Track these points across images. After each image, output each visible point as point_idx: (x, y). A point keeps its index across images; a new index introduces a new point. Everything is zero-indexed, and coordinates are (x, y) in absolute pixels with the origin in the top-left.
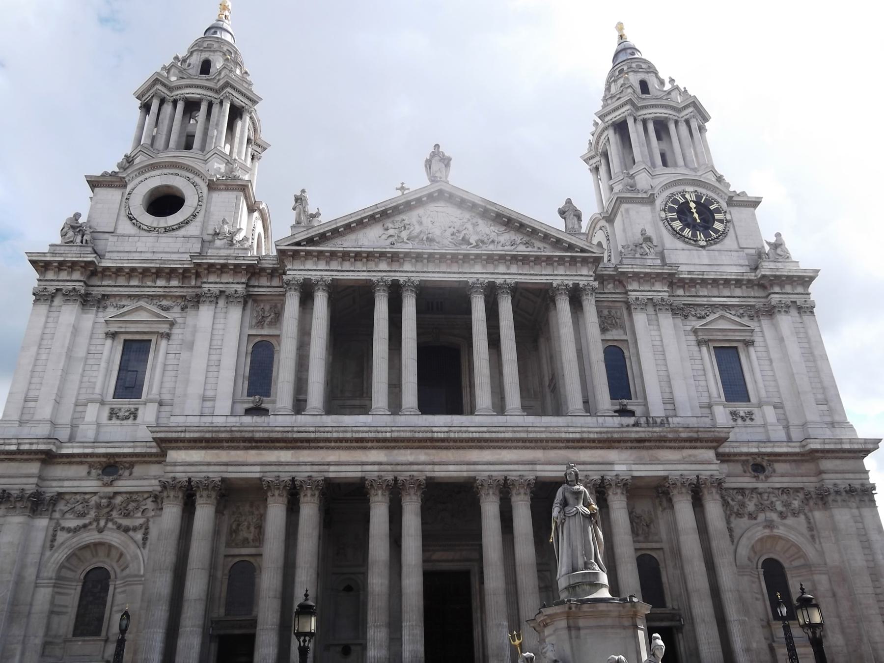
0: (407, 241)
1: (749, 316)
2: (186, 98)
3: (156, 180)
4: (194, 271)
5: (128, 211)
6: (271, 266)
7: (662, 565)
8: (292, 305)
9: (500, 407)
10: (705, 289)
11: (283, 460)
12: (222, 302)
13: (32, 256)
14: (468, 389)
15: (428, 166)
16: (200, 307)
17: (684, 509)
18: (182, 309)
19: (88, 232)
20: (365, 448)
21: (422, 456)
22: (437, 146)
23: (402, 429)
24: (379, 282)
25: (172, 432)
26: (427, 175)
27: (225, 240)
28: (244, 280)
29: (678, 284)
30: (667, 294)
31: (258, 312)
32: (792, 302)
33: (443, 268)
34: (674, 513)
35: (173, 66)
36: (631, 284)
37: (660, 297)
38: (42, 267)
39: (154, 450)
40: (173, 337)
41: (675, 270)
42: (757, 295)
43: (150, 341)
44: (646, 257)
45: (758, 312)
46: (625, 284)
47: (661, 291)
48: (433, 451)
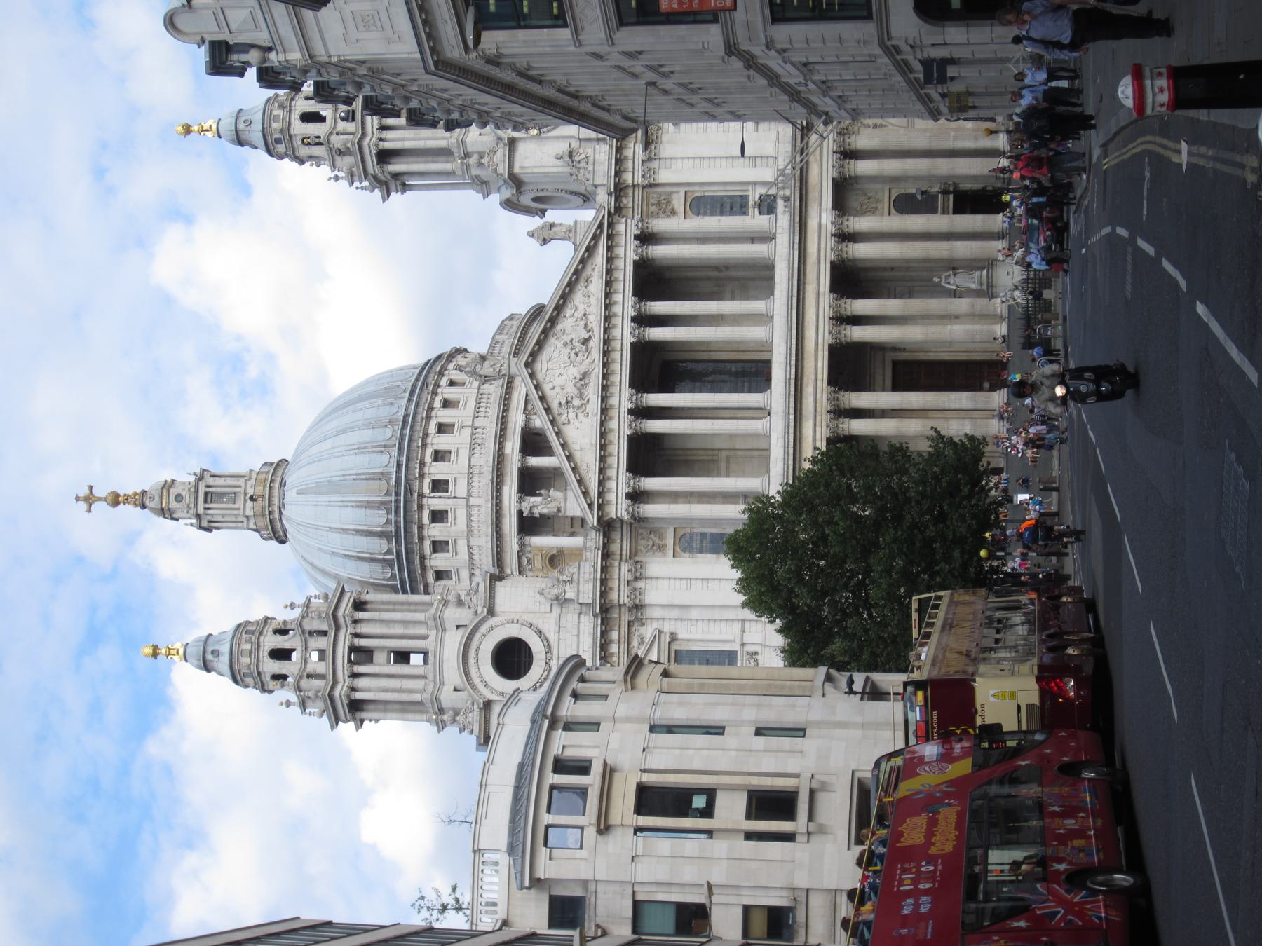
4: (604, 614)
6: (601, 538)
7: (903, 191)
8: (651, 510)
14: (712, 353)
16: (647, 602)
17: (863, 167)
18: (643, 624)
21: (809, 390)
28: (617, 564)
30: (637, 145)
33: (616, 367)
34: (861, 177)
36: (624, 180)
40: (672, 631)
44: (591, 159)
46: (624, 186)
48: (805, 380)
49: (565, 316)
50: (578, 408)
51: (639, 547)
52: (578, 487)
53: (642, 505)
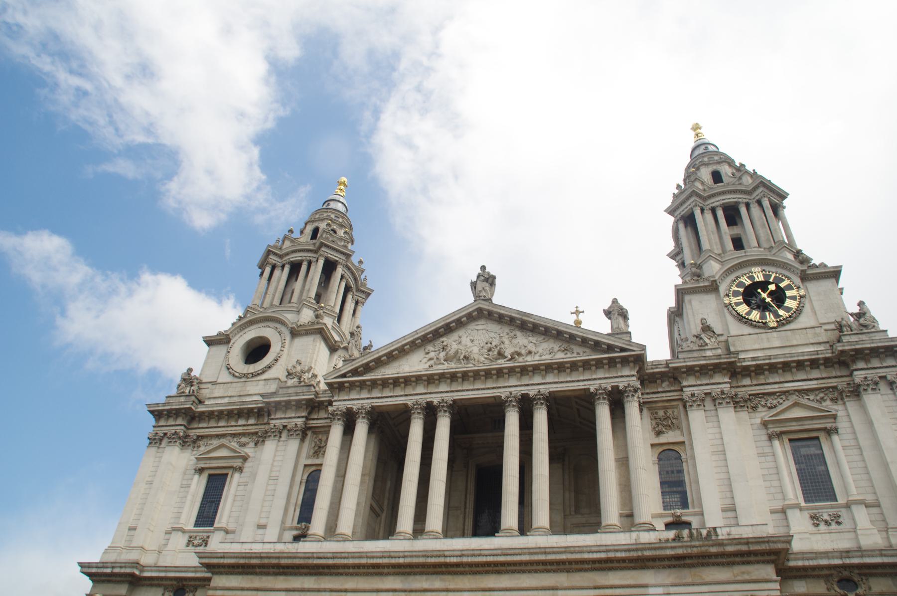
0: (445, 363)
1: (832, 400)
2: (291, 261)
3: (252, 333)
4: (266, 410)
5: (227, 362)
6: (327, 399)
8: (336, 432)
9: (525, 527)
10: (776, 375)
11: (306, 586)
12: (284, 435)
13: (150, 407)
15: (474, 289)
18: (256, 444)
19: (195, 383)
20: (381, 574)
22: (483, 268)
23: (414, 554)
24: (414, 405)
25: (214, 558)
26: (474, 296)
27: (296, 380)
28: (304, 414)
29: (744, 373)
30: (728, 385)
31: (316, 442)
32: (881, 377)
35: (285, 238)
36: (686, 379)
37: (720, 390)
38: (157, 415)
39: (209, 575)
40: (245, 470)
41: (734, 358)
42: (839, 374)
43: (227, 475)
44: (706, 347)
45: (841, 393)
46: (680, 380)
47: (722, 384)
48: (449, 577)
49: (529, 337)
50: (437, 358)
51: (320, 437)
52: (361, 363)
53: (341, 422)
